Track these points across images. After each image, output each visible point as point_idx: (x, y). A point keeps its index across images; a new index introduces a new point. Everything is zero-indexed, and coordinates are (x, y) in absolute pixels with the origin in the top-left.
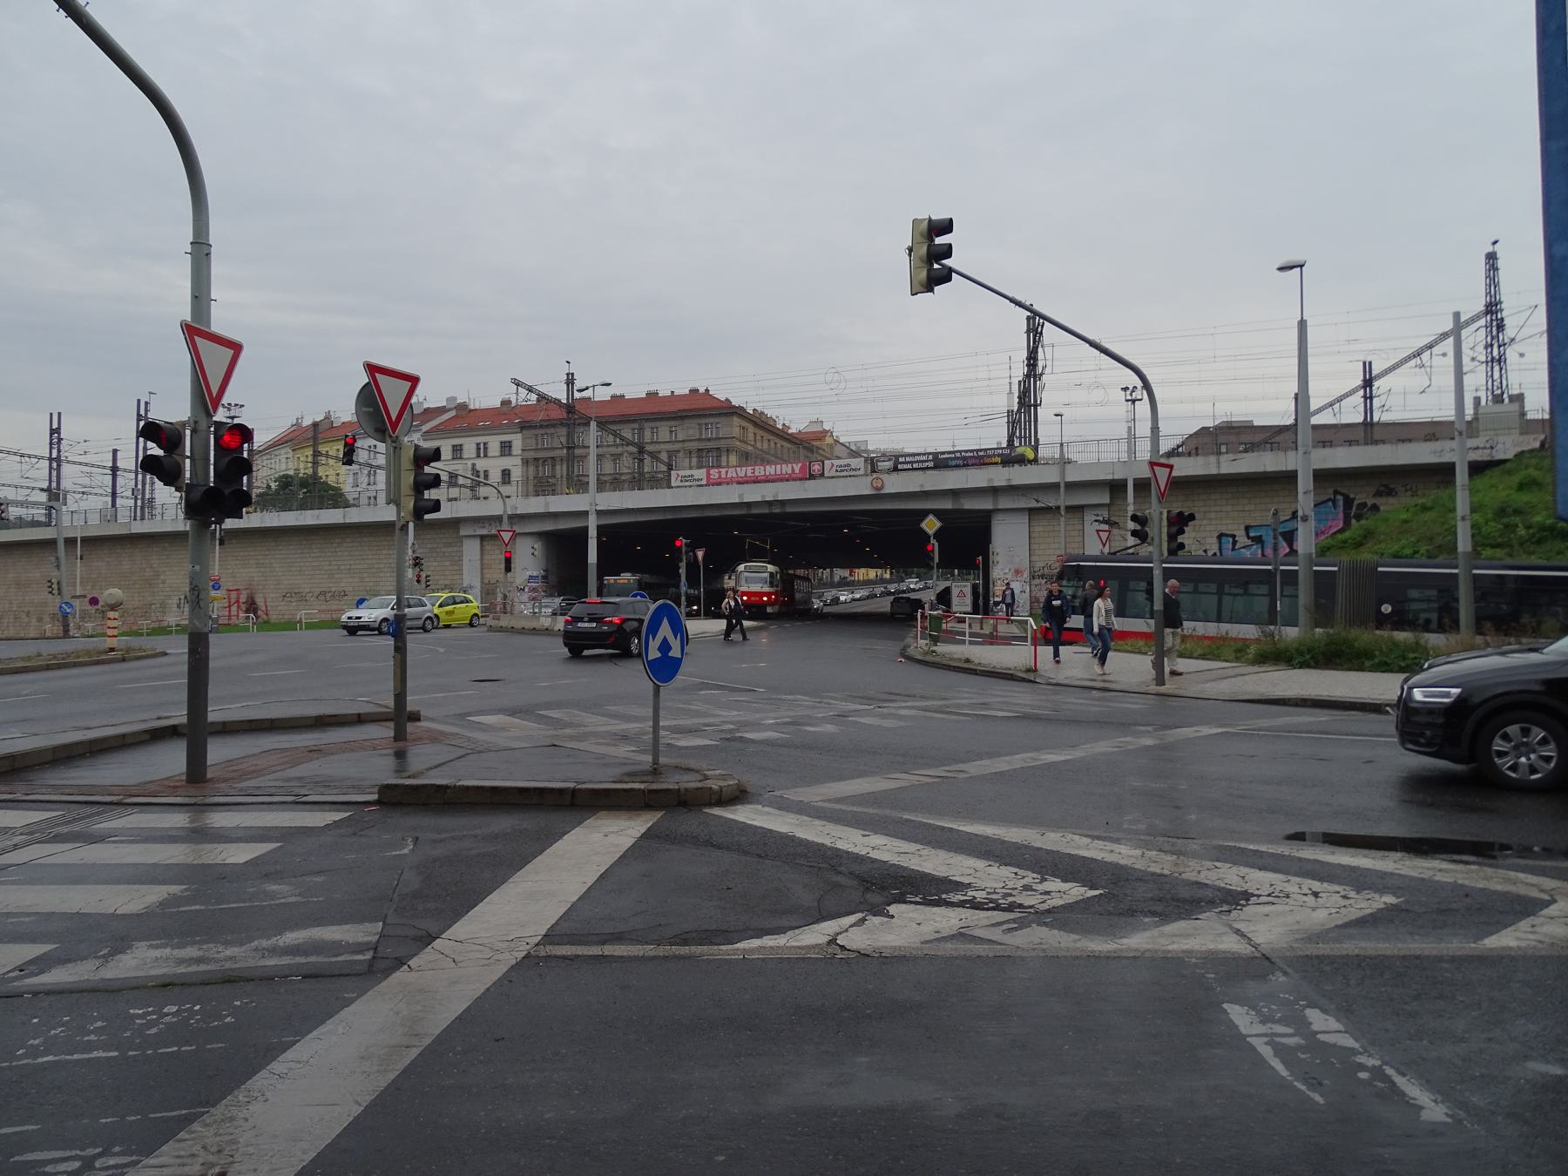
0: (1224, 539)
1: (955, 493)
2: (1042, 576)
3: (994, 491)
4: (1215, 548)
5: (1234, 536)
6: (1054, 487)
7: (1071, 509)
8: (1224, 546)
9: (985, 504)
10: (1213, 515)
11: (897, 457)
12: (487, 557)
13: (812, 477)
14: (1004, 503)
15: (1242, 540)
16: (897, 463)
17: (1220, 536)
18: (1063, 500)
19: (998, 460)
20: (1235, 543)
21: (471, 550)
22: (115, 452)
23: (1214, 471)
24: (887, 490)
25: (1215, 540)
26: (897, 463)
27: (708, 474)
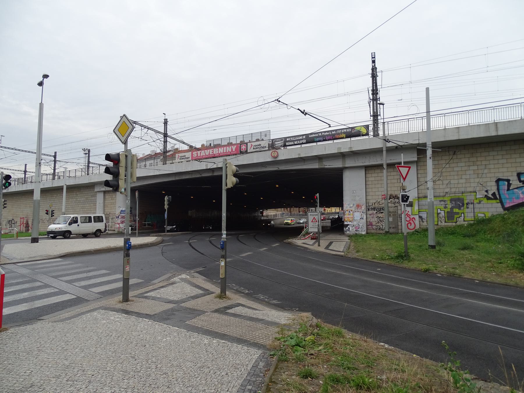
0: (501, 183)
1: (319, 158)
2: (374, 209)
3: (343, 156)
4: (494, 189)
5: (508, 181)
6: (377, 152)
7: (391, 166)
8: (501, 187)
9: (337, 164)
10: (492, 166)
11: (286, 138)
12: (106, 201)
13: (241, 153)
14: (349, 163)
15: (515, 183)
16: (286, 141)
17: (498, 181)
18: (384, 160)
19: (344, 136)
20: (509, 185)
21: (100, 197)
22: (26, 165)
23: (493, 134)
24: (281, 157)
25: (494, 184)
26: (286, 141)
27: (192, 155)
